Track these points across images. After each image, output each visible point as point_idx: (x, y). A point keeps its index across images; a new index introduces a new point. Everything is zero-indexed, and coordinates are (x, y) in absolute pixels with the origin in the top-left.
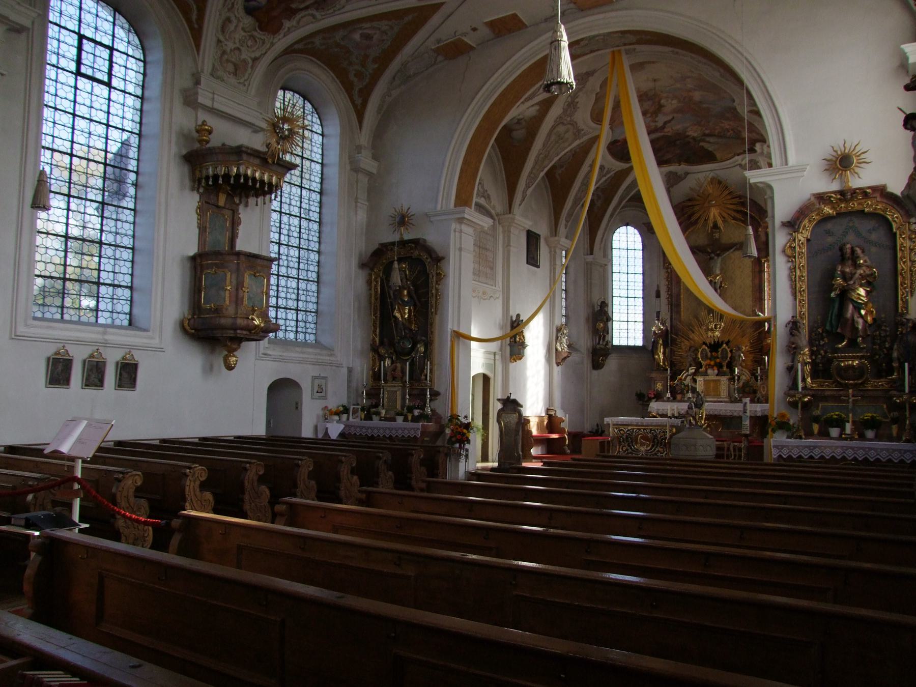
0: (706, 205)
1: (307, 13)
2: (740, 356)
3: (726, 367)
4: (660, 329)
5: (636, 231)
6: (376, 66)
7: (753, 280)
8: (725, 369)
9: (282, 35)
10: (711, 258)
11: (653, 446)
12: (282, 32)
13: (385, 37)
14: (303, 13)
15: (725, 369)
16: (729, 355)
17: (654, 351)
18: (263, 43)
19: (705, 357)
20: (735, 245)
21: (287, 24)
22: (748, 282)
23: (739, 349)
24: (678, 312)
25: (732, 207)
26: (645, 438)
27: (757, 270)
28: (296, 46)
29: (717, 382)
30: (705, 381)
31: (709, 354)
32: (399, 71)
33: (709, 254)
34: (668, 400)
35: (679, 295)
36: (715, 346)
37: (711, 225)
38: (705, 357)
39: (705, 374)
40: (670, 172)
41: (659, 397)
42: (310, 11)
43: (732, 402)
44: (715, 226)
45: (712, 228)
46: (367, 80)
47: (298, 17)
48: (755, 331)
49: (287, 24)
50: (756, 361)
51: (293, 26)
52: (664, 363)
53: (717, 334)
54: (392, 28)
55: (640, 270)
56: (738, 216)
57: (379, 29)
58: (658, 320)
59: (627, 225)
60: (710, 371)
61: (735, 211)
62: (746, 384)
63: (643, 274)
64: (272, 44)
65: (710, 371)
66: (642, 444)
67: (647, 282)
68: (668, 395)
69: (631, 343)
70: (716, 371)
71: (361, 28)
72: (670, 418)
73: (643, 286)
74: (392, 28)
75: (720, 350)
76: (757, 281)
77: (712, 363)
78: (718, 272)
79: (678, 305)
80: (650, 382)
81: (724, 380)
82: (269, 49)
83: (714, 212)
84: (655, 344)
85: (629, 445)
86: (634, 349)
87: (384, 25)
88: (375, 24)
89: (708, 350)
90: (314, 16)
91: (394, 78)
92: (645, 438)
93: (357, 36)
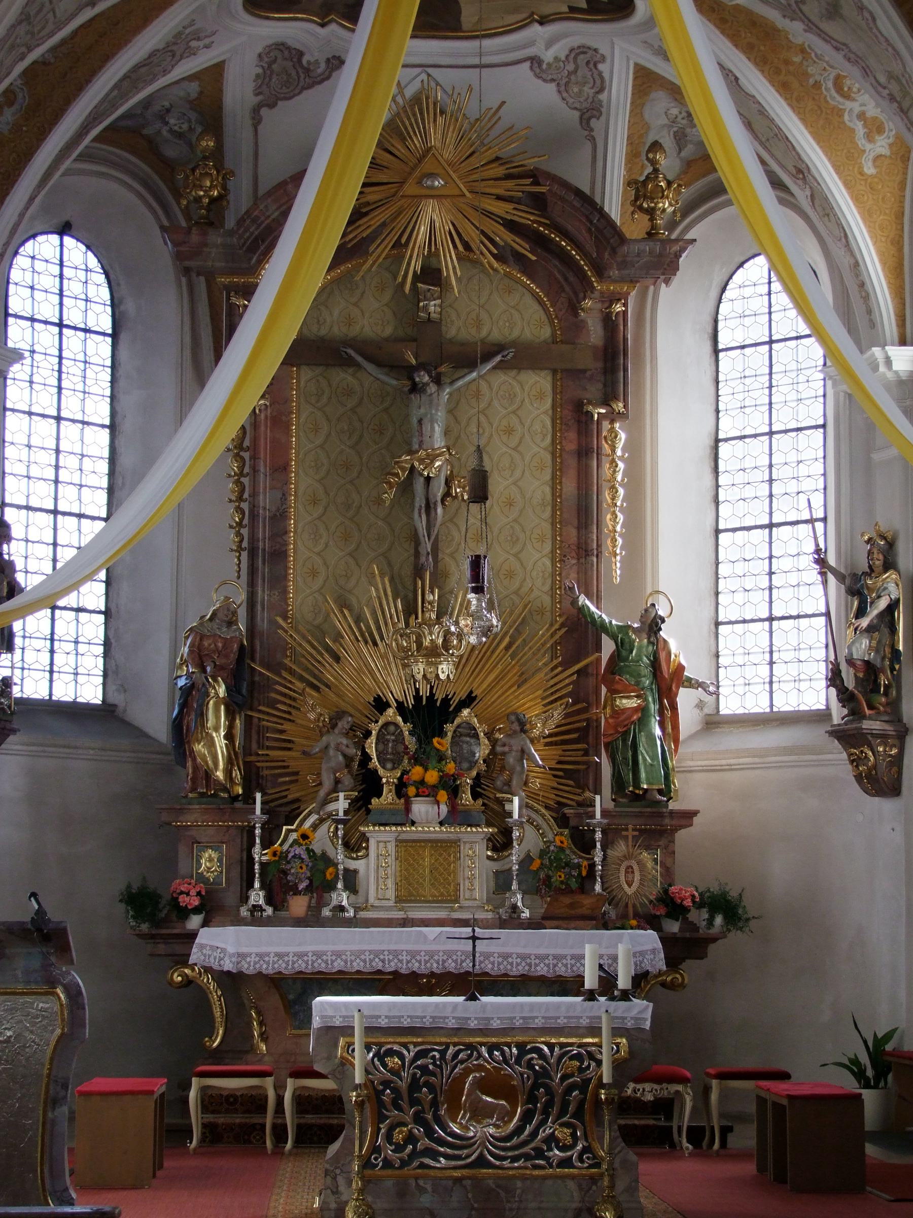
0: (410, 188)
2: (523, 753)
3: (480, 797)
4: (487, 631)
5: (93, 262)
7: (555, 482)
8: (466, 797)
10: (415, 388)
11: (527, 1117)
15: (466, 797)
16: (482, 751)
17: (184, 729)
19: (390, 758)
20: (499, 348)
22: (538, 487)
23: (523, 726)
24: (279, 581)
25: (502, 209)
26: (493, 1084)
27: (572, 446)
29: (446, 848)
30: (400, 842)
31: (411, 742)
33: (409, 371)
34: (256, 918)
35: (280, 517)
36: (430, 714)
37: (416, 265)
38: (390, 758)
39: (405, 818)
40: (281, 47)
41: (213, 909)
43: (503, 924)
44: (431, 274)
45: (416, 278)
48: (566, 664)
50: (569, 774)
52: (228, 772)
53: (445, 670)
55: (101, 411)
56: (521, 246)
58: (478, 590)
59: (64, 230)
60: (421, 808)
61: (511, 226)
62: (551, 858)
63: (113, 427)
65: (421, 808)
66: (479, 1113)
67: (126, 460)
68: (257, 896)
69: (64, 692)
70: (444, 809)
72: (591, 996)
73: (112, 474)
75: (449, 728)
76: (569, 486)
77: (432, 777)
78: (439, 441)
79: (279, 555)
80: (172, 842)
81: (474, 841)
83: (433, 217)
84: (190, 700)
85: (419, 1119)
86: (74, 712)
89: (406, 728)
92: (493, 1084)
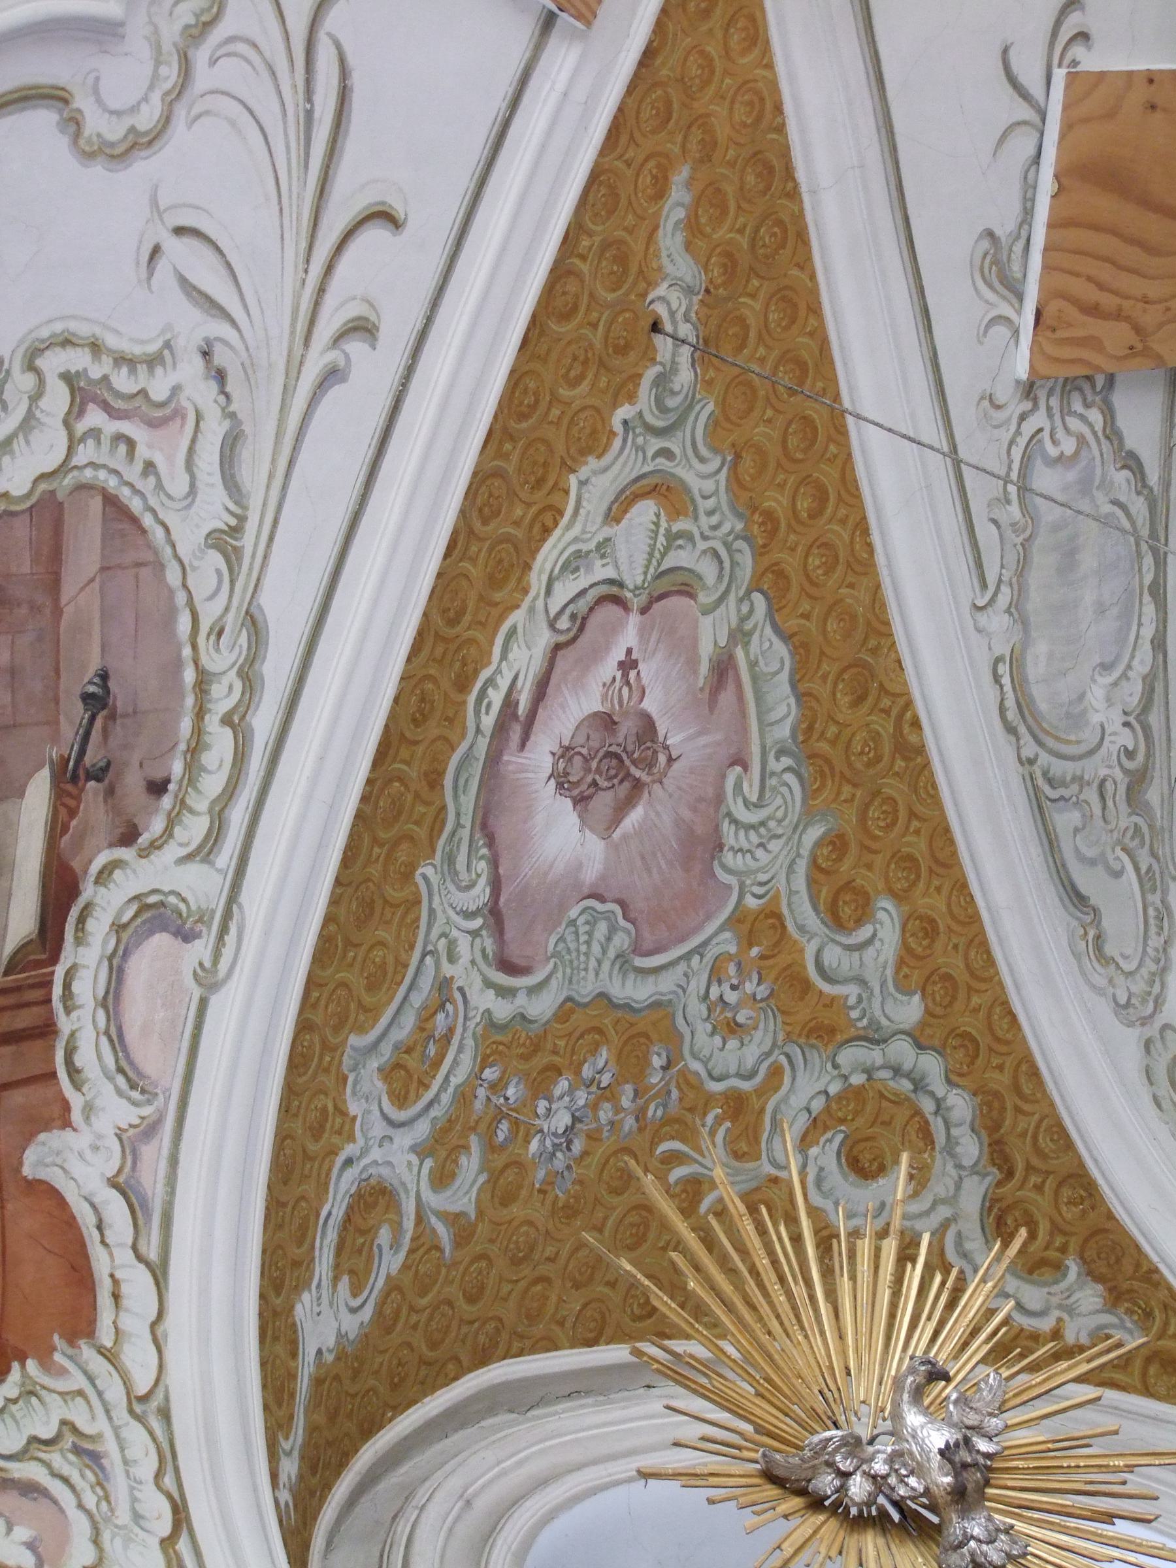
1: (99, 927)
6: (886, 927)
9: (138, 1284)
12: (113, 1259)
13: (710, 635)
14: (85, 960)
18: (91, 1457)
21: (77, 1162)
28: (328, 1320)
32: (1039, 806)
42: (107, 902)
46: (961, 1105)
47: (81, 1024)
49: (77, 1162)
51: (133, 1141)
54: (664, 490)
57: (613, 596)
64: (151, 1406)
71: (516, 723)
74: (664, 490)
82: (168, 1458)
87: (597, 532)
88: (554, 579)
90: (156, 915)
91: (1076, 898)
93: (559, 838)
